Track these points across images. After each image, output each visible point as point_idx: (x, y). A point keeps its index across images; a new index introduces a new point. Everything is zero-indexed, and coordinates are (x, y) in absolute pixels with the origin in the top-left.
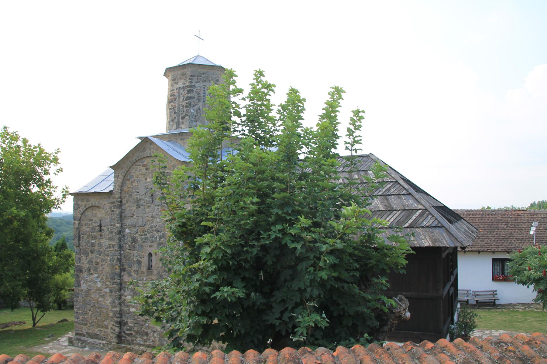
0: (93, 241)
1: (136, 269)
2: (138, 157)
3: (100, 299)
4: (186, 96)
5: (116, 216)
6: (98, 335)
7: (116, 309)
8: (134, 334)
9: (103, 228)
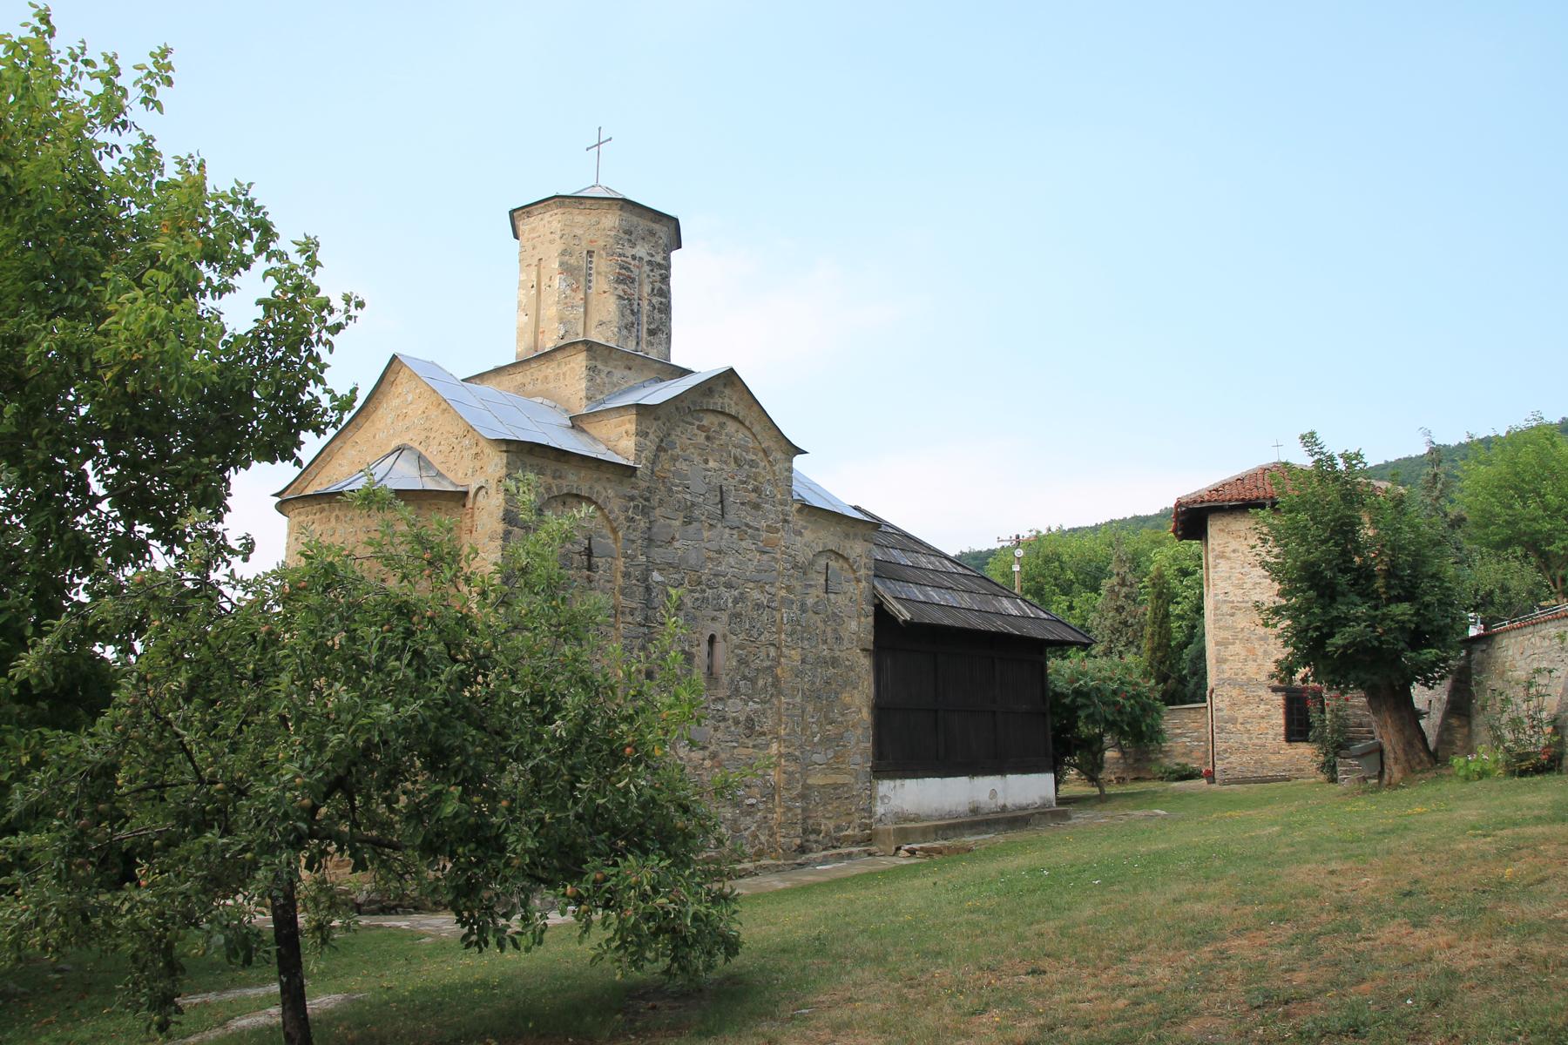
2: (694, 403)
4: (657, 285)
5: (638, 533)
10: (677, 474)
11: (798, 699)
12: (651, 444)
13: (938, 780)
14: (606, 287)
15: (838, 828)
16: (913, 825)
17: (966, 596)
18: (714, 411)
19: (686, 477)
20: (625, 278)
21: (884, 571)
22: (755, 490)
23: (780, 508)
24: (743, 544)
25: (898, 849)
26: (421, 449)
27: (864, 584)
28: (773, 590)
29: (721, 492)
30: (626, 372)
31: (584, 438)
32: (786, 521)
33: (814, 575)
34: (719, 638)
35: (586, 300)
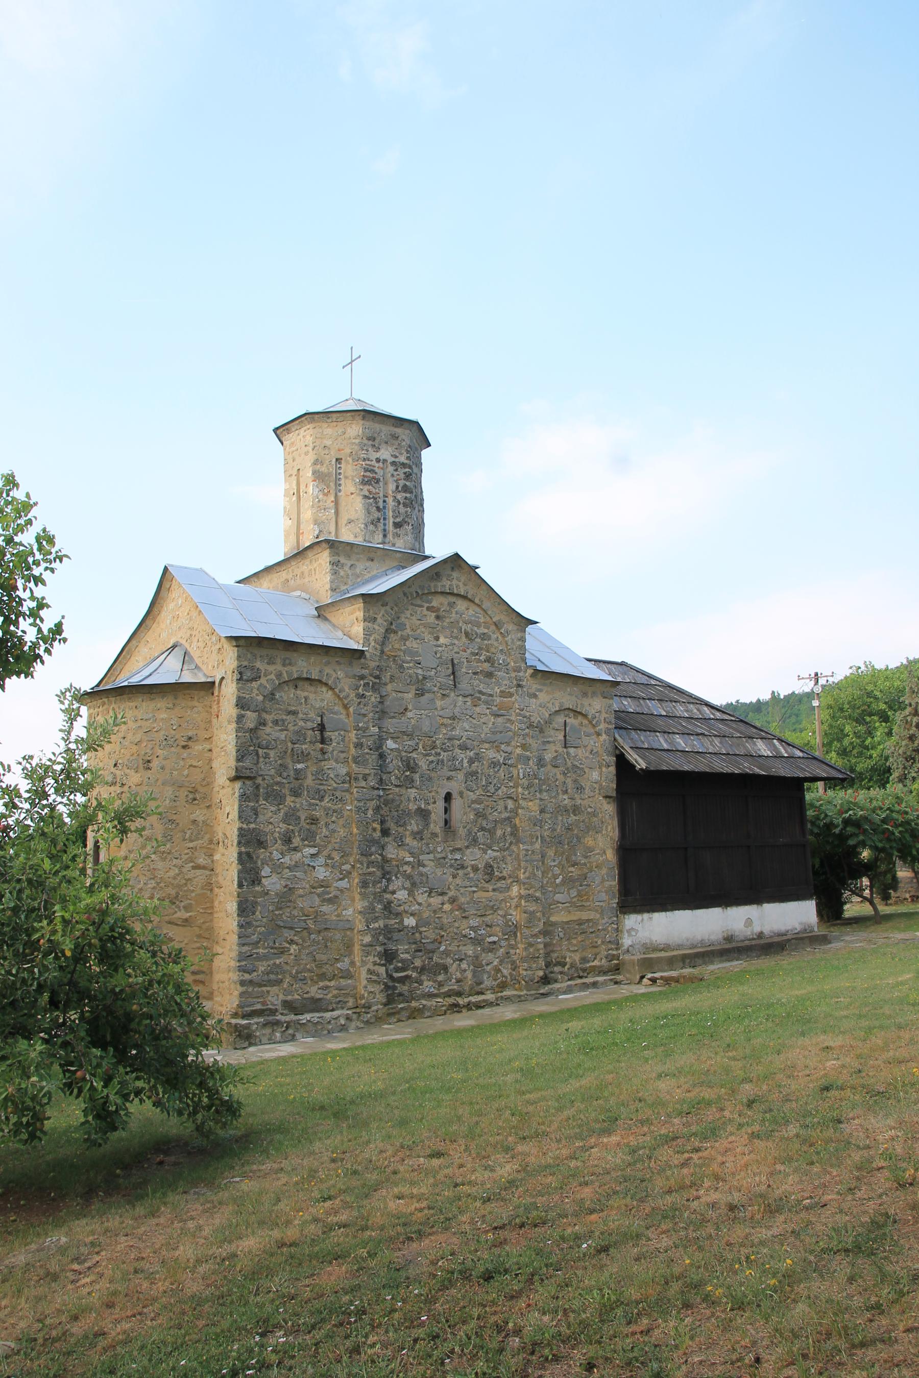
0: (299, 766)
1: (415, 829)
2: (422, 588)
3: (325, 908)
4: (402, 483)
5: (369, 708)
6: (320, 999)
7: (377, 925)
8: (414, 975)
9: (327, 734)
10: (408, 652)
11: (537, 846)
12: (379, 629)
13: (688, 912)
14: (353, 489)
15: (584, 960)
16: (663, 954)
17: (717, 741)
18: (442, 593)
19: (417, 654)
20: (370, 479)
21: (624, 722)
22: (488, 660)
23: (513, 675)
24: (478, 709)
25: (642, 977)
26: (187, 645)
27: (604, 736)
28: (509, 749)
29: (453, 665)
30: (369, 564)
31: (325, 626)
32: (519, 686)
33: (552, 732)
34: (455, 795)
35: (336, 502)
